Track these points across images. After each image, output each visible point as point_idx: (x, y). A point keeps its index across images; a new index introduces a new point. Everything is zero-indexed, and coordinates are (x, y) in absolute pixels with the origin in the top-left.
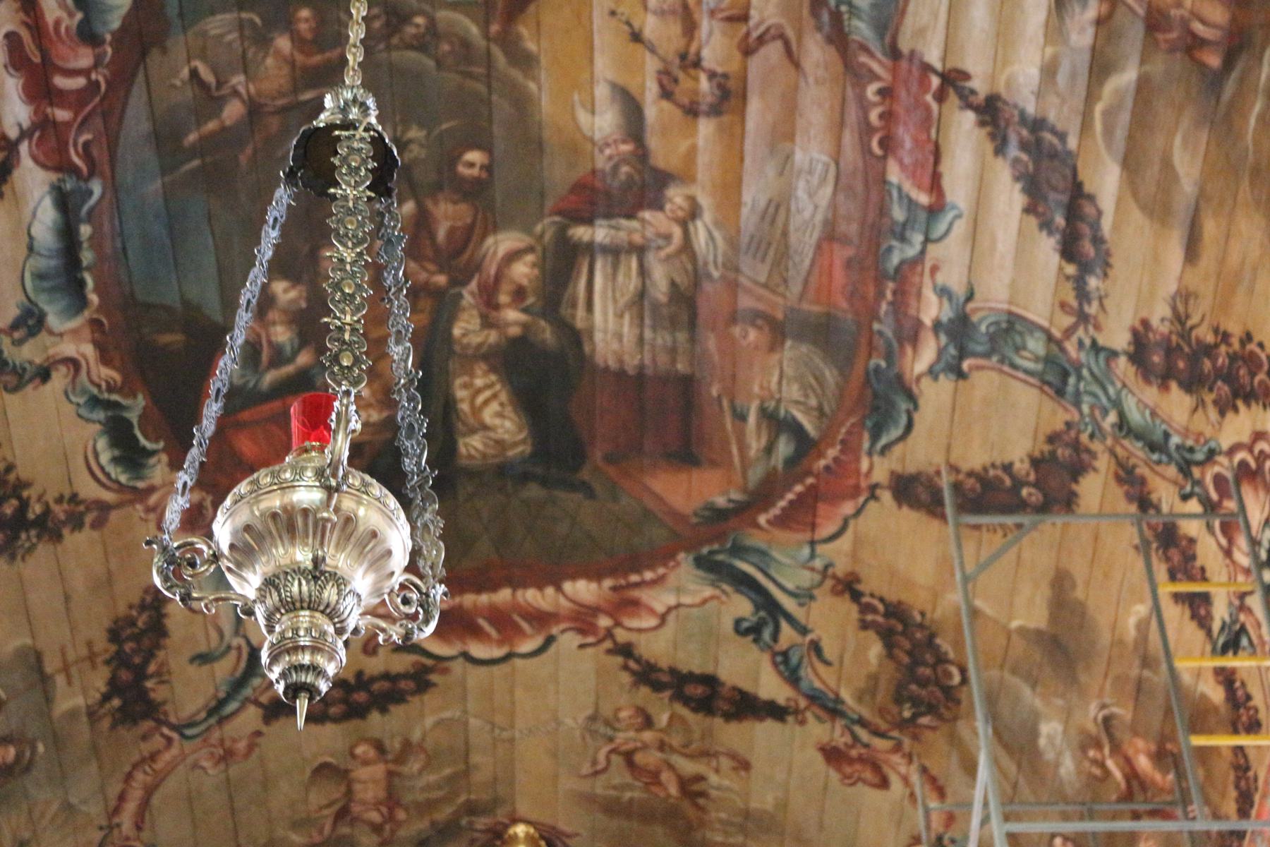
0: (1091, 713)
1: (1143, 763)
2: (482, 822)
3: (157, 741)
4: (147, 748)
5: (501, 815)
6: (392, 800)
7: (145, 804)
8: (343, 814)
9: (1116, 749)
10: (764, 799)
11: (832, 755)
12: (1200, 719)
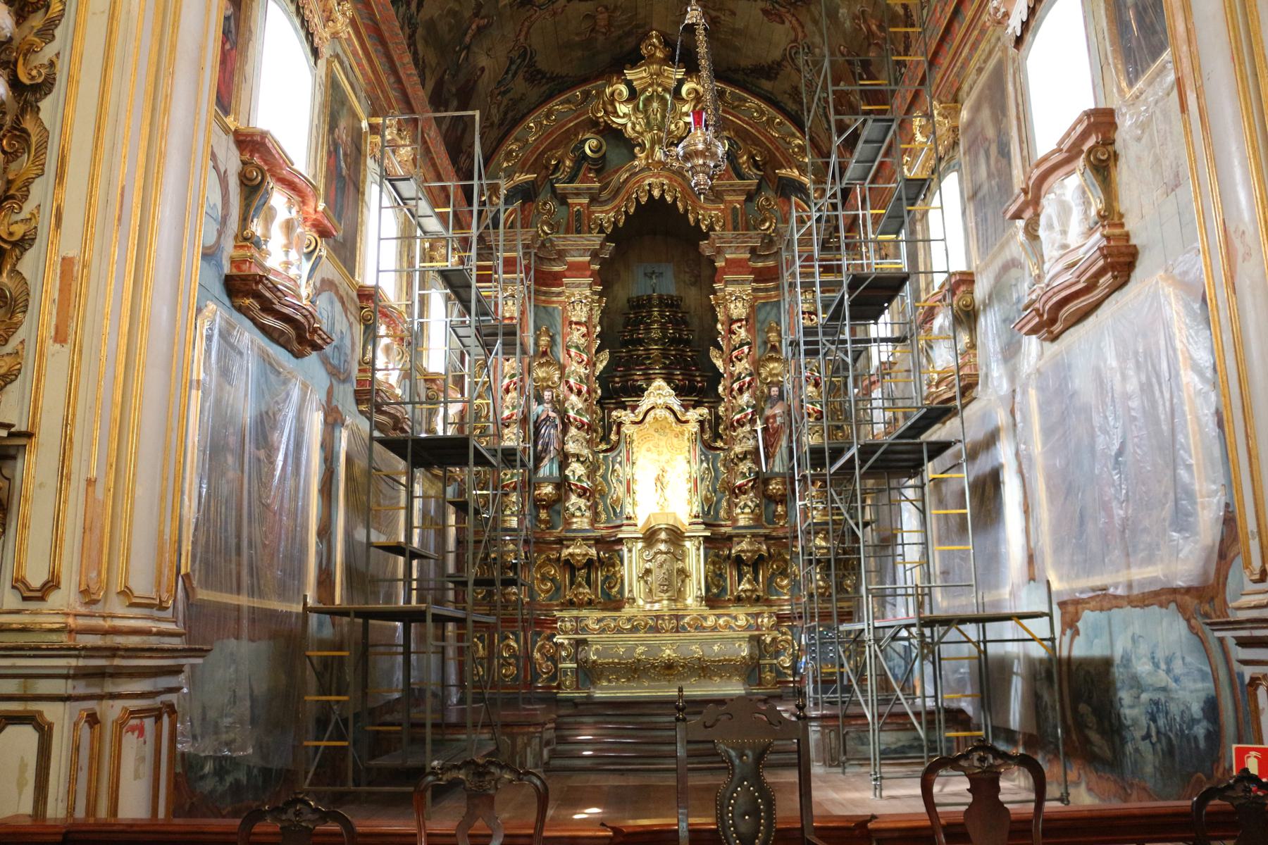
0: (857, 9)
1: (874, 27)
2: (640, 31)
3: (532, 12)
4: (528, 14)
5: (647, 28)
6: (610, 25)
7: (527, 33)
8: (592, 30)
9: (865, 21)
10: (740, 25)
11: (765, 12)
12: (894, 20)
